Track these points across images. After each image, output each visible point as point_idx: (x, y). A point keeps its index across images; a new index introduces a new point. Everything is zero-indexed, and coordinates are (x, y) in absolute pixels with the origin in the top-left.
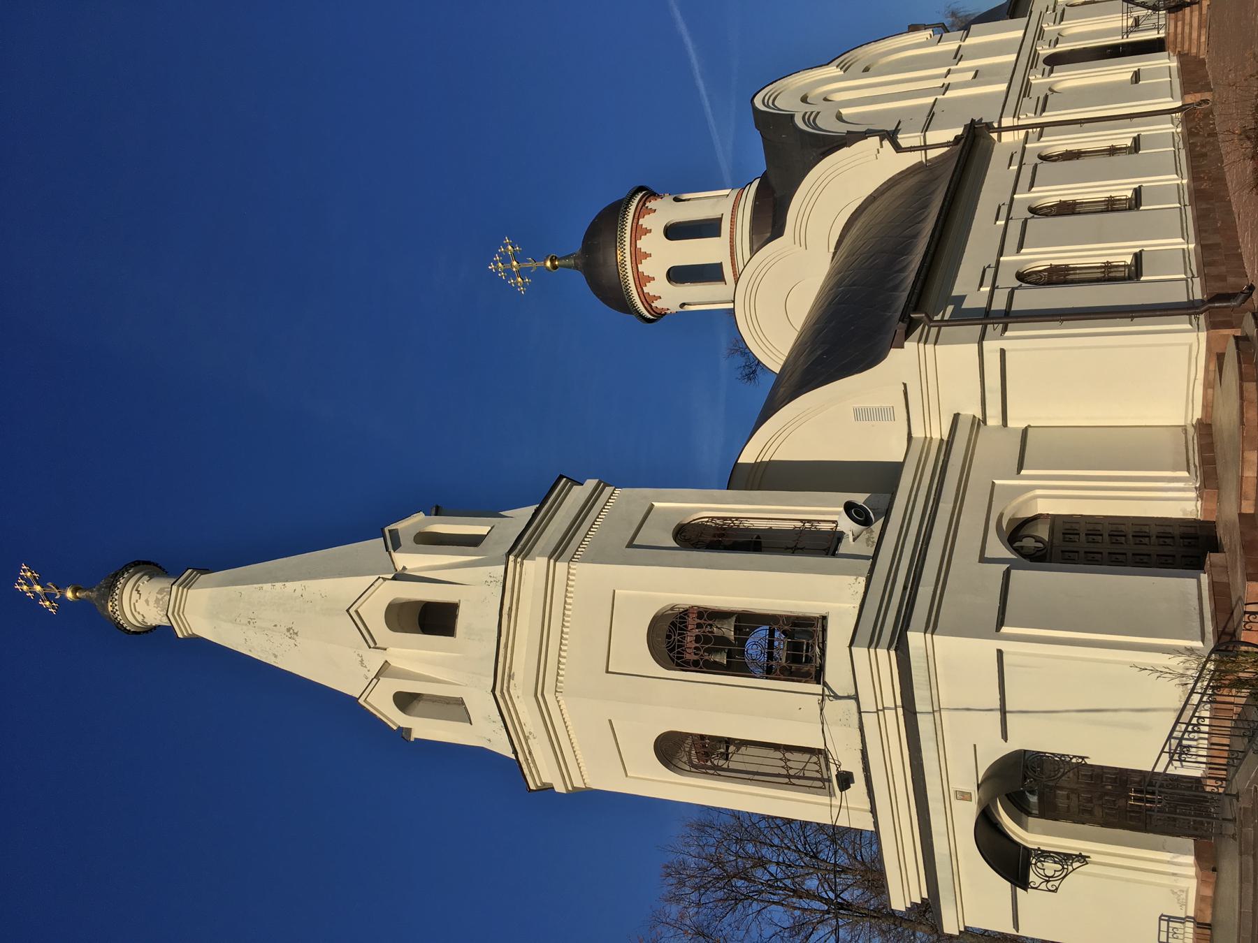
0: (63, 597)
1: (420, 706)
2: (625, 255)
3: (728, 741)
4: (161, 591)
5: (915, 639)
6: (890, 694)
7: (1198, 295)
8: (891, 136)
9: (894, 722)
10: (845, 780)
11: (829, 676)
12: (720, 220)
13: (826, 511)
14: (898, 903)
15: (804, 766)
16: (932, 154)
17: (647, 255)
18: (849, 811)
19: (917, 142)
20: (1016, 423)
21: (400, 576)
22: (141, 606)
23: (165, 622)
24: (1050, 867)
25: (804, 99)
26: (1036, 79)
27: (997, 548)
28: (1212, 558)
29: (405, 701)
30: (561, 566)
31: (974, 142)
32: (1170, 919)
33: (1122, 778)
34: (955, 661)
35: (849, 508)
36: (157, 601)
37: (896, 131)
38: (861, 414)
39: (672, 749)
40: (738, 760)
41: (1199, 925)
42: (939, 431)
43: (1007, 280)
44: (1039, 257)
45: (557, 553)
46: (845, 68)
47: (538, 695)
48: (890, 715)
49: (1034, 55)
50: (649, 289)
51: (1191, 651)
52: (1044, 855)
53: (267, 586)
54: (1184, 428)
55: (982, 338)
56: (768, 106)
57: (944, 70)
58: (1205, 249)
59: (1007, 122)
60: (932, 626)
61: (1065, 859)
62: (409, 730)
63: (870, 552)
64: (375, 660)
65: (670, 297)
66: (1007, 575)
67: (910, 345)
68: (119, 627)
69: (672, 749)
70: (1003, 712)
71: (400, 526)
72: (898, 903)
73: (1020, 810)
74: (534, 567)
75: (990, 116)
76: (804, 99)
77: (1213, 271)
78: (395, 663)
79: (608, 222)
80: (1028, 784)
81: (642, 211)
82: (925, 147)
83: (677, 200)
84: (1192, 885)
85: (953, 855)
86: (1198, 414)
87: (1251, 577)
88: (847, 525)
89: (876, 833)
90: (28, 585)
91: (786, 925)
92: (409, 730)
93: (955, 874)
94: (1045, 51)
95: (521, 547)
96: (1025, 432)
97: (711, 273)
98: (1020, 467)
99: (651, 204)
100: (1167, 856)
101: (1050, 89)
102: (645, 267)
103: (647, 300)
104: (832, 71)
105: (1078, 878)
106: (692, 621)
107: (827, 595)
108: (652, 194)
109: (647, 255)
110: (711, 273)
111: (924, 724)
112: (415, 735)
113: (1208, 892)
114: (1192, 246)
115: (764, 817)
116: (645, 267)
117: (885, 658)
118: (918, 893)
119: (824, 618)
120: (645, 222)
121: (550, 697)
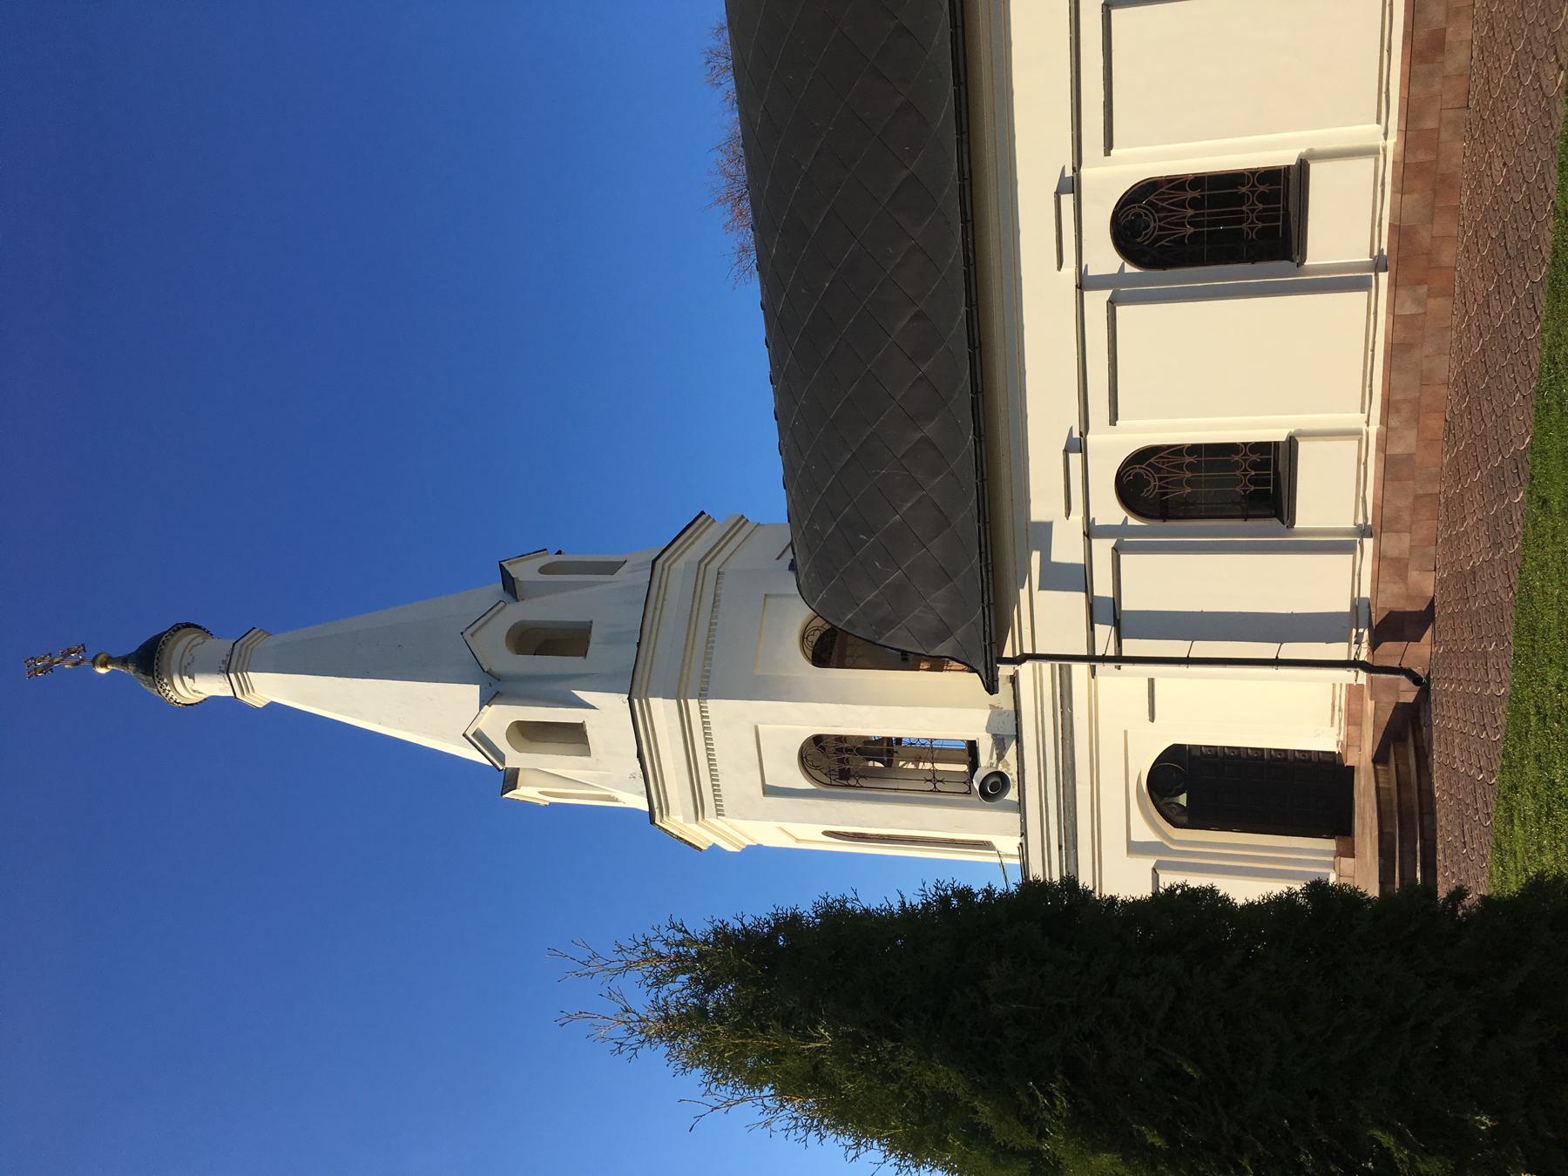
7: (1366, 592)
27: (1144, 832)
30: (714, 821)
98: (1152, 719)
114: (1374, 429)
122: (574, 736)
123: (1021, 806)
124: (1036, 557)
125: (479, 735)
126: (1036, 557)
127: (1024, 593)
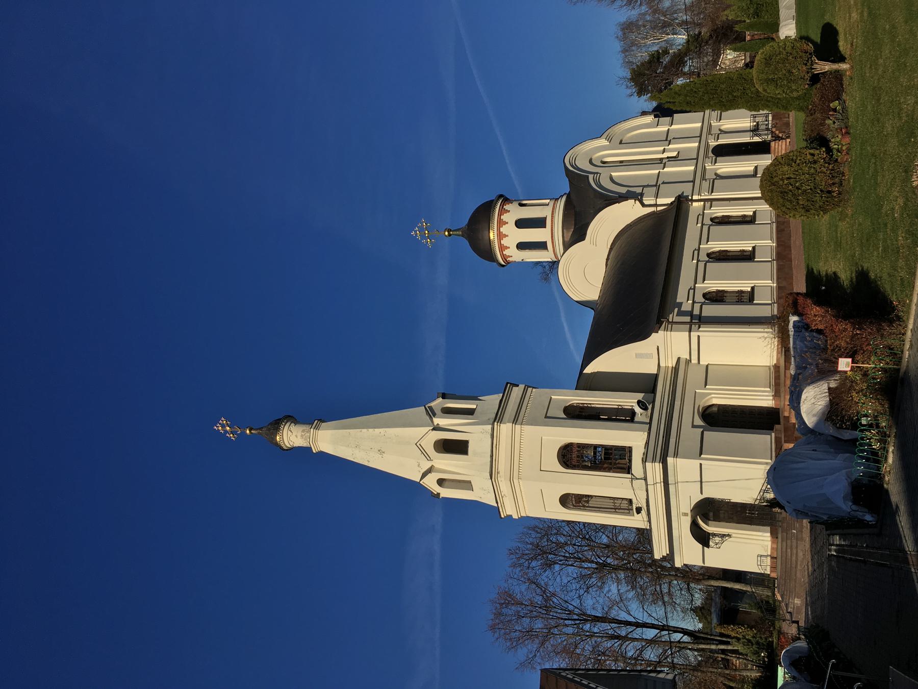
0: (244, 433)
1: (446, 483)
2: (493, 235)
3: (588, 496)
4: (303, 431)
5: (670, 460)
6: (659, 477)
7: (776, 313)
8: (639, 197)
9: (660, 488)
10: (639, 510)
11: (634, 471)
12: (545, 218)
13: (629, 401)
14: (657, 556)
15: (625, 506)
16: (659, 208)
17: (506, 236)
18: (637, 521)
19: (653, 202)
20: (704, 362)
21: (437, 428)
22: (293, 438)
23: (305, 445)
24: (717, 539)
25: (591, 162)
26: (709, 166)
27: (699, 421)
28: (777, 427)
29: (441, 482)
30: (518, 427)
31: (681, 203)
32: (761, 556)
33: (743, 507)
34: (683, 468)
35: (639, 402)
36: (302, 436)
37: (642, 194)
38: (638, 356)
39: (566, 500)
40: (591, 503)
41: (772, 558)
42: (672, 363)
43: (699, 298)
44: (712, 285)
45: (515, 421)
46: (609, 139)
47: (511, 480)
48: (658, 485)
49: (707, 145)
50: (506, 252)
51: (767, 463)
52: (714, 535)
53: (364, 430)
54: (769, 367)
55: (690, 331)
56: (572, 166)
57: (662, 148)
58: (780, 288)
59: (695, 197)
60: (676, 455)
61: (723, 536)
62: (439, 494)
63: (648, 421)
64: (426, 465)
65: (517, 256)
66: (702, 433)
67: (661, 332)
68: (281, 448)
69: (566, 500)
70: (701, 482)
71: (432, 404)
72: (657, 556)
73: (706, 519)
74: (505, 429)
75: (686, 189)
76: (591, 162)
77: (782, 301)
78: (436, 466)
79: (483, 215)
80: (710, 510)
81: (502, 211)
82: (656, 205)
83: (521, 205)
84: (769, 544)
85: (680, 537)
86: (775, 362)
87: (786, 442)
88: (638, 410)
89: (651, 529)
90: (223, 427)
91: (575, 576)
92: (439, 494)
93: (680, 543)
94: (713, 143)
95: (498, 418)
96: (707, 366)
97: (542, 246)
98: (706, 385)
99: (507, 207)
100: (760, 534)
101: (716, 174)
102: (504, 242)
103: (504, 257)
104: (603, 142)
105: (728, 543)
106: (575, 449)
107: (633, 439)
108: (506, 200)
109: (506, 236)
110: (542, 246)
111: (672, 489)
112: (441, 496)
113: (775, 546)
115: (563, 521)
116: (504, 242)
117: (658, 466)
118: (665, 551)
119: (630, 449)
120: (504, 217)
121: (516, 481)
122: (470, 412)
123: (650, 423)
124: (676, 310)
125: (430, 408)
126: (676, 310)
127: (671, 316)
